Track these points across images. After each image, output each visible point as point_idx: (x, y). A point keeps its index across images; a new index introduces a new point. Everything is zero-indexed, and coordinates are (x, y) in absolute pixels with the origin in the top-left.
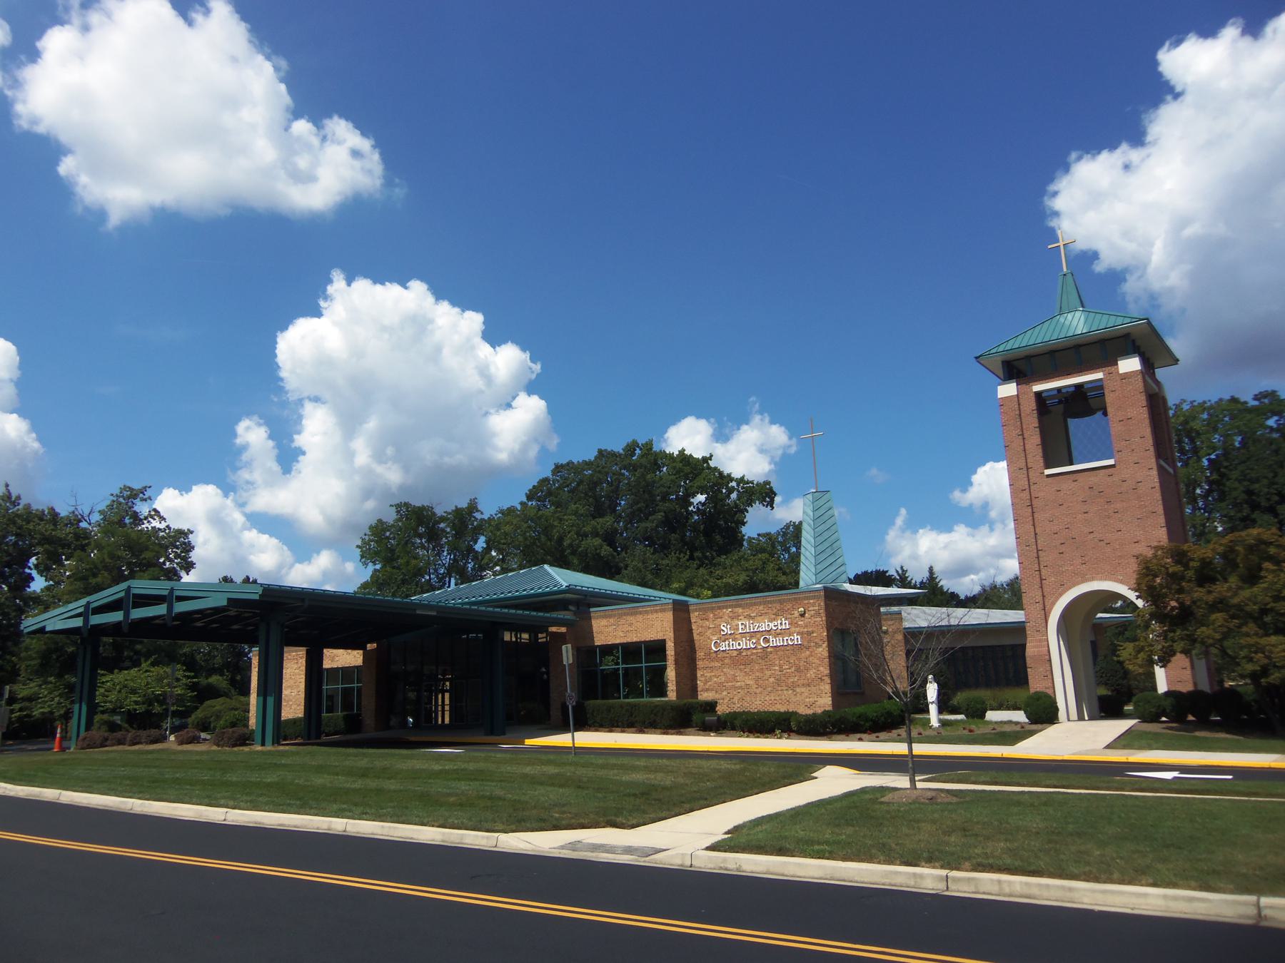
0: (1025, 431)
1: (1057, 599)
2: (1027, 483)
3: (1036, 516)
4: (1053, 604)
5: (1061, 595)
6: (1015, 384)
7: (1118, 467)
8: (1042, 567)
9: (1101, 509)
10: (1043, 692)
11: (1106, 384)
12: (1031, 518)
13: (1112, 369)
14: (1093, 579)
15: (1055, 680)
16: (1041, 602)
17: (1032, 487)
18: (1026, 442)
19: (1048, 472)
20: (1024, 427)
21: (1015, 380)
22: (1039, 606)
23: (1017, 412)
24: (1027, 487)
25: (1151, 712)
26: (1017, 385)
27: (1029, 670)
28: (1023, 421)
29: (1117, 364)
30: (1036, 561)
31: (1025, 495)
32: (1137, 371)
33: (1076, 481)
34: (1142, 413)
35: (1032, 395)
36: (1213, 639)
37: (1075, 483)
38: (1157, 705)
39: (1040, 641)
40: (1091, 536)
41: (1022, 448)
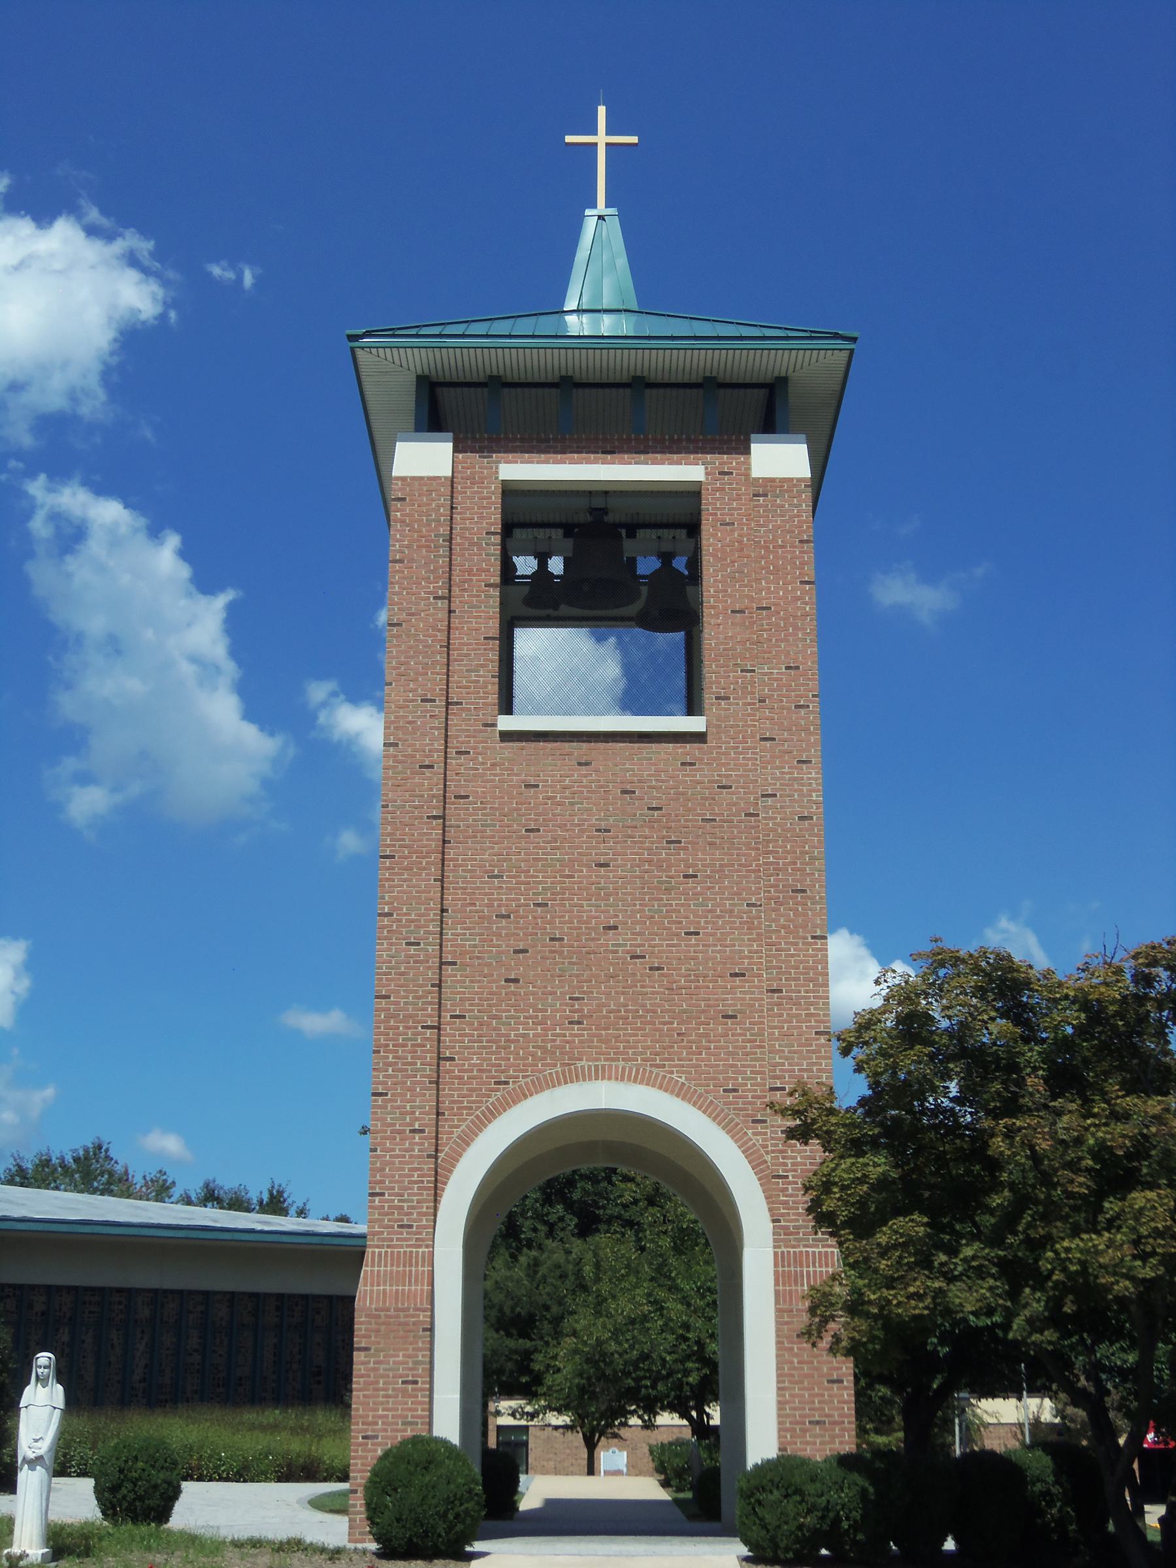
0: (456, 590)
1: (480, 1125)
2: (439, 745)
3: (451, 853)
4: (466, 1141)
5: (492, 1114)
6: (449, 446)
7: (712, 742)
8: (446, 1016)
9: (650, 861)
10: (404, 1443)
11: (707, 500)
12: (435, 857)
13: (731, 461)
14: (599, 1074)
15: (436, 1396)
16: (429, 1131)
17: (452, 762)
18: (455, 622)
19: (506, 723)
20: (456, 579)
21: (451, 434)
22: (421, 1145)
23: (444, 530)
24: (437, 757)
25: (801, 1527)
26: (456, 450)
27: (358, 1357)
28: (457, 559)
29: (747, 451)
30: (432, 998)
31: (430, 783)
32: (800, 480)
33: (587, 764)
34: (798, 598)
35: (495, 488)
36: (1132, 1279)
37: (584, 770)
38: (822, 1501)
39: (409, 1259)
40: (611, 938)
41: (441, 636)
